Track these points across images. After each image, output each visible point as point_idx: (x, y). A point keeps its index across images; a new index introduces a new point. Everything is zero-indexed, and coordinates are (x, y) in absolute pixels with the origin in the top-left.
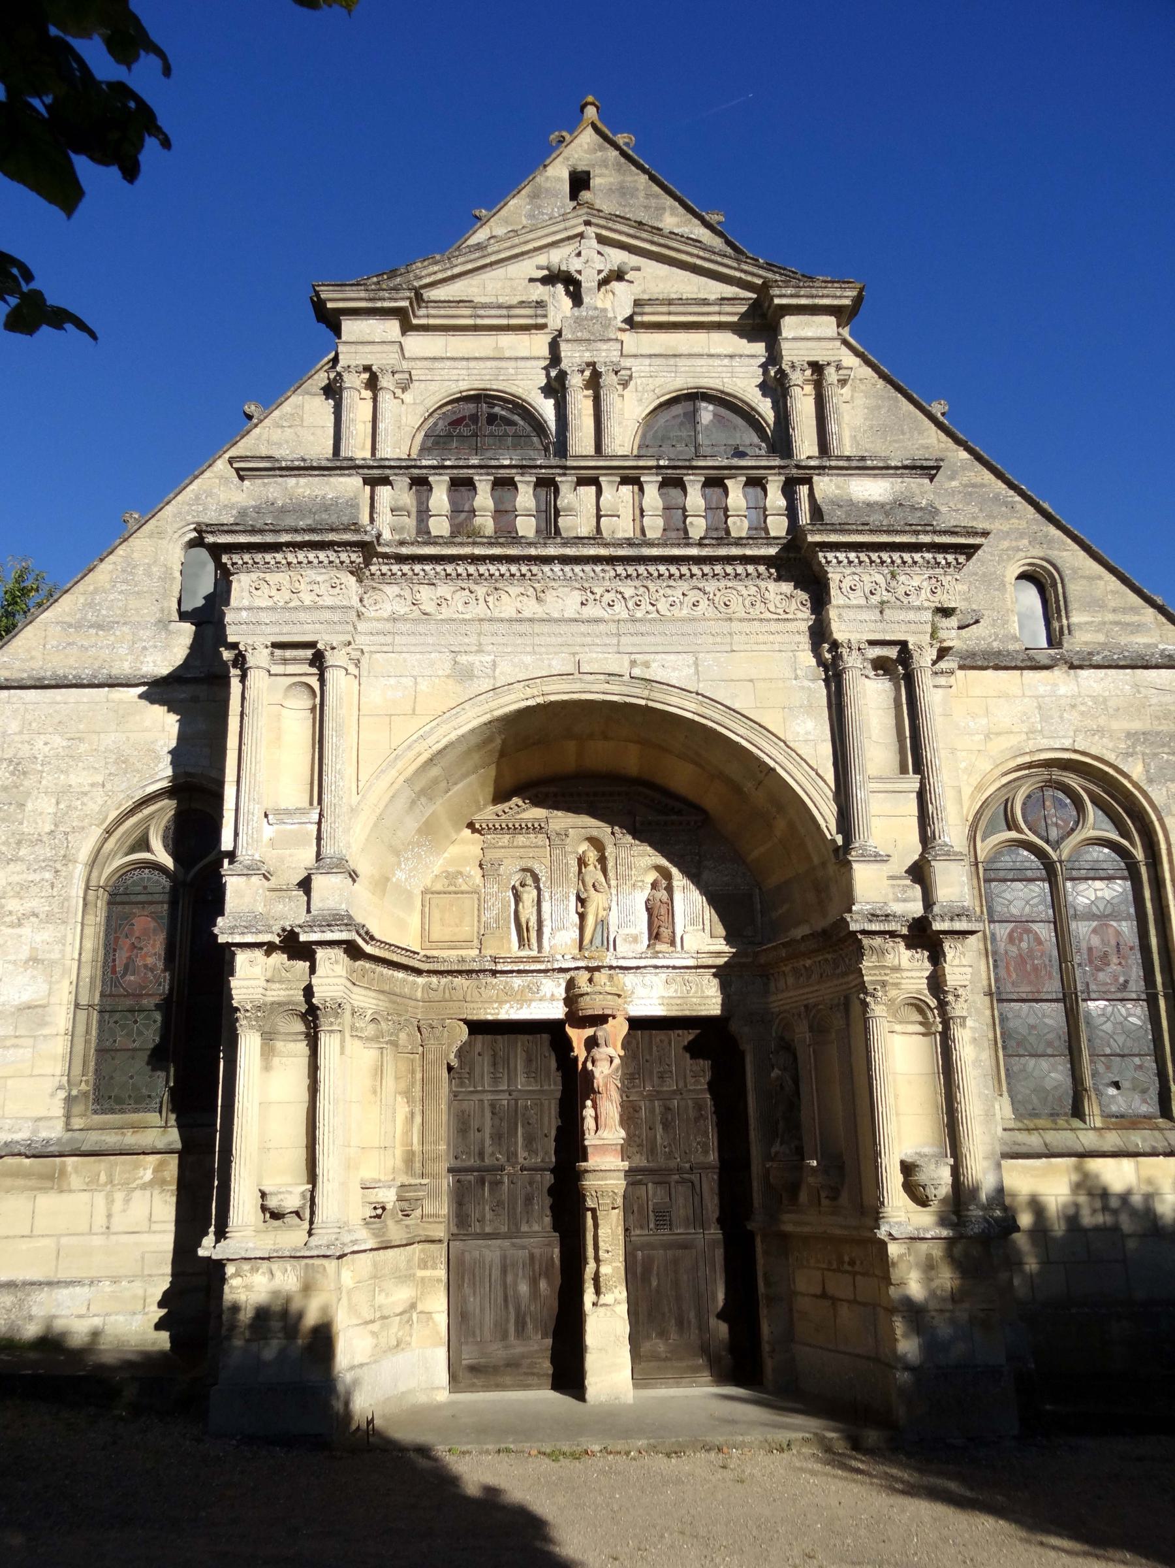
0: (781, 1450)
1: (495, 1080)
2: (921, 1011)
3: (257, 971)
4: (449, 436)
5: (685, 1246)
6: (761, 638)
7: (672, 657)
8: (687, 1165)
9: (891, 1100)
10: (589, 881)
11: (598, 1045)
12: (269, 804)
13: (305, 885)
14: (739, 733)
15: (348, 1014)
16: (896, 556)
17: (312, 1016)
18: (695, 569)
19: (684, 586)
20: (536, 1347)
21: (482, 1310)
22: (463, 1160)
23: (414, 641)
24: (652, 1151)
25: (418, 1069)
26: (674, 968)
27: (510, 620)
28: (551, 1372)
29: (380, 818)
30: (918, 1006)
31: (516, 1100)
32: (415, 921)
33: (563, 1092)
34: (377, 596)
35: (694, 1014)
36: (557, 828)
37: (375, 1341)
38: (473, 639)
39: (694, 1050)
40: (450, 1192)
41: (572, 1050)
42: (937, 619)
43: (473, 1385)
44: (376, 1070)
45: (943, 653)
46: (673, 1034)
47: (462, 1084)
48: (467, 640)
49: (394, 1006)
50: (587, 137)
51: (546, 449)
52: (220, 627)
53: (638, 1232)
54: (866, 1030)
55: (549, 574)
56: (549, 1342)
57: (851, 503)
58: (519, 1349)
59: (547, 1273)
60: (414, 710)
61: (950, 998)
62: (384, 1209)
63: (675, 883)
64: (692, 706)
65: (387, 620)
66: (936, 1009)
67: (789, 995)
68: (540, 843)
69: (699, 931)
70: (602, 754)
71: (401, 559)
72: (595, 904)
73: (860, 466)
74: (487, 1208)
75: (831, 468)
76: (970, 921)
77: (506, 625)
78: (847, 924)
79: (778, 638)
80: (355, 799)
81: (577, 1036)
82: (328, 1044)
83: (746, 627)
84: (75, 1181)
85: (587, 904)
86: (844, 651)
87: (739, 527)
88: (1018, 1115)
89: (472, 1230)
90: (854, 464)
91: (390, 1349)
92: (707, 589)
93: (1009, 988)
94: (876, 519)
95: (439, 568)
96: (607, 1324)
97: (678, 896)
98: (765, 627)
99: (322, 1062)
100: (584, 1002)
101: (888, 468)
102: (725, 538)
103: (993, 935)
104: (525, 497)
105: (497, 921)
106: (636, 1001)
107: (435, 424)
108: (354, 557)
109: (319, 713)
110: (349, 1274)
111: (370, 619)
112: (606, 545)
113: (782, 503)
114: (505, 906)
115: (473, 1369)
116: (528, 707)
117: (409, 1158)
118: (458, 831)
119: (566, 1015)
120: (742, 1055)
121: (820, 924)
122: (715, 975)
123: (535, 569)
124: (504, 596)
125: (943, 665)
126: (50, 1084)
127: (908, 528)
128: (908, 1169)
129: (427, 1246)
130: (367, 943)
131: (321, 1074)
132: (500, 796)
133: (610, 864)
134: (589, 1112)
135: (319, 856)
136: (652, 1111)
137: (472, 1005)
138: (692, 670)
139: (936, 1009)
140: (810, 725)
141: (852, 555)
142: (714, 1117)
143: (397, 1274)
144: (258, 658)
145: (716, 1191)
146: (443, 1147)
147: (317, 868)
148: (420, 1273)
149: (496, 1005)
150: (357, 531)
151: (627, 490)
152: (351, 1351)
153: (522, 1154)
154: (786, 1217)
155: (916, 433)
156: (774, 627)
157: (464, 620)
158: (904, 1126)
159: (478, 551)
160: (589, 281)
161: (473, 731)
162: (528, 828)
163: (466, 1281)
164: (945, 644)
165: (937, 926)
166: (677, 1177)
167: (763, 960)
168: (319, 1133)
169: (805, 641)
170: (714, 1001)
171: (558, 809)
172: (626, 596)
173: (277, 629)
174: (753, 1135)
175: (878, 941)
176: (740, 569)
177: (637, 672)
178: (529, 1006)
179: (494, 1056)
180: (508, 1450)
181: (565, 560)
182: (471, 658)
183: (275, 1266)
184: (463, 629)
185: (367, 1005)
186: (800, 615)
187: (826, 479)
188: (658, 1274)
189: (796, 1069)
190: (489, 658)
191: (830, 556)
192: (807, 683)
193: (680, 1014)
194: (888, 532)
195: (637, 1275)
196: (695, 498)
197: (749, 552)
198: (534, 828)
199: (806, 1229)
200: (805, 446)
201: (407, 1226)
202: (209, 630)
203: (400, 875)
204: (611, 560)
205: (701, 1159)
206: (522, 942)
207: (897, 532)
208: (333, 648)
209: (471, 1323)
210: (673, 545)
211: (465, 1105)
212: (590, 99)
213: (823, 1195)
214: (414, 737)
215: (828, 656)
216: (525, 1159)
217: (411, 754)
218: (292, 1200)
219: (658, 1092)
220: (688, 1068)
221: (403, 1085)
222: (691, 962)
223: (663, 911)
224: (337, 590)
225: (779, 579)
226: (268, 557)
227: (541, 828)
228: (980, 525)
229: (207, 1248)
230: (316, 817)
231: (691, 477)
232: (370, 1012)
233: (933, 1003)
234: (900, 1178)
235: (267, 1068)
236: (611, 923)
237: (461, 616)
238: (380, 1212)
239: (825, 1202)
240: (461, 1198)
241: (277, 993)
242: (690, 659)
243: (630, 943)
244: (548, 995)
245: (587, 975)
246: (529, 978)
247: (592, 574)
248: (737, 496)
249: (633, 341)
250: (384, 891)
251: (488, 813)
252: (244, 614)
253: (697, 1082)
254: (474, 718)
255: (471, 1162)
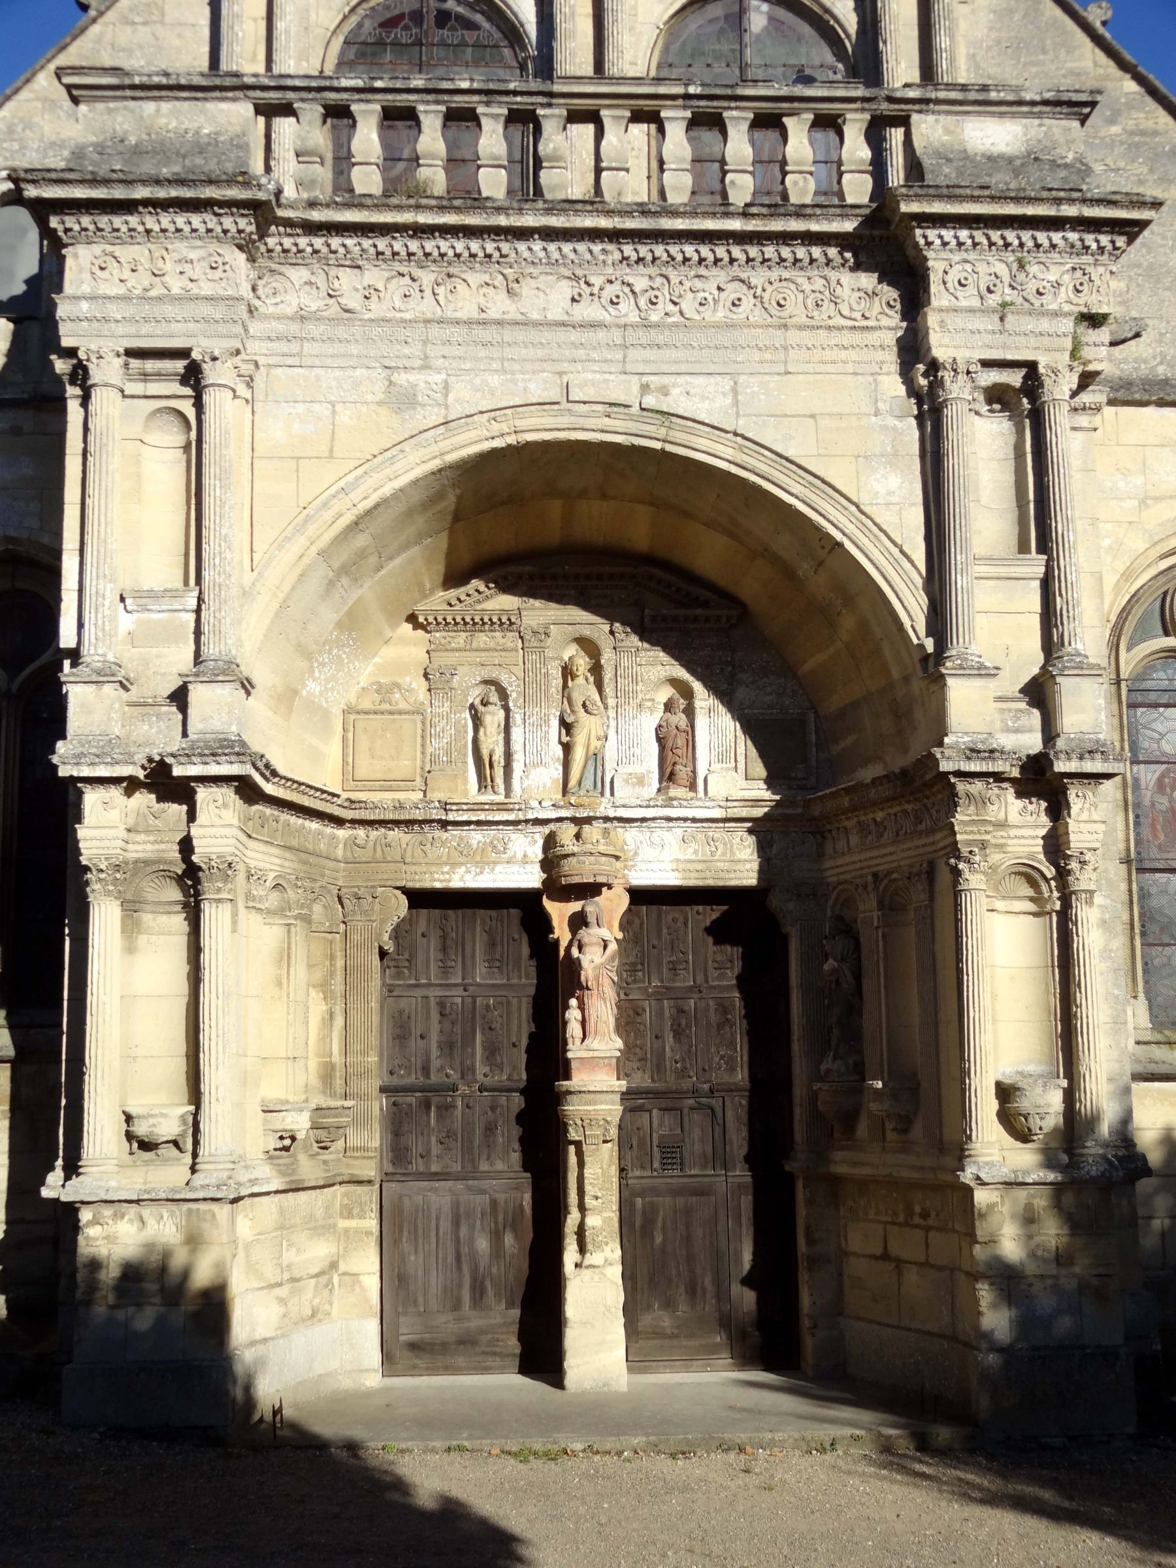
0: (823, 1450)
1: (445, 970)
2: (1032, 883)
3: (114, 816)
4: (380, 43)
5: (700, 1192)
6: (828, 355)
7: (701, 380)
8: (706, 1087)
9: (986, 1001)
10: (578, 699)
11: (586, 924)
12: (126, 583)
13: (180, 697)
14: (792, 492)
15: (241, 877)
16: (1026, 236)
17: (190, 878)
18: (737, 252)
19: (719, 276)
20: (498, 1320)
21: (426, 1271)
22: (402, 1077)
23: (331, 351)
24: (659, 1067)
25: (339, 954)
26: (694, 820)
27: (469, 323)
28: (518, 1351)
29: (284, 606)
30: (1030, 876)
31: (474, 998)
32: (334, 750)
33: (538, 987)
34: (276, 283)
35: (720, 883)
36: (534, 624)
37: (282, 1310)
38: (415, 350)
39: (719, 932)
40: (383, 1118)
41: (552, 931)
42: (1082, 328)
43: (415, 1367)
44: (281, 953)
45: (1087, 380)
46: (690, 911)
47: (399, 975)
48: (407, 351)
49: (305, 868)
51: (523, 67)
52: (50, 325)
53: (637, 1173)
54: (957, 907)
55: (526, 254)
56: (516, 1313)
57: (965, 156)
58: (476, 1322)
59: (514, 1225)
60: (331, 451)
61: (1074, 865)
62: (293, 1139)
63: (698, 704)
64: (728, 452)
65: (292, 319)
66: (1054, 881)
67: (851, 859)
68: (510, 645)
69: (730, 770)
70: (597, 520)
71: (312, 228)
72: (585, 731)
73: (980, 100)
74: (433, 1139)
75: (938, 102)
76: (1106, 760)
77: (464, 330)
78: (936, 762)
79: (853, 355)
80: (248, 578)
81: (559, 912)
82: (214, 917)
83: (807, 337)
85: (575, 731)
86: (946, 375)
87: (801, 189)
88: (1157, 1024)
89: (413, 1168)
90: (972, 96)
91: (303, 1320)
92: (754, 281)
93: (1154, 853)
94: (1000, 180)
95: (366, 243)
96: (594, 1291)
97: (701, 722)
98: (836, 338)
99: (206, 941)
100: (568, 866)
101: (1020, 103)
102: (779, 205)
103: (1136, 780)
104: (492, 139)
105: (448, 753)
106: (641, 866)
107: (360, 25)
108: (243, 223)
109: (195, 453)
110: (247, 1224)
111: (267, 317)
112: (609, 213)
113: (866, 153)
114: (462, 732)
115: (413, 1347)
116: (494, 452)
117: (327, 1074)
118: (394, 626)
119: (543, 883)
120: (785, 940)
121: (898, 762)
122: (750, 831)
123: (505, 247)
124: (461, 287)
125: (1086, 398)
127: (1045, 194)
128: (1005, 1093)
129: (352, 1188)
130: (267, 780)
131: (206, 958)
132: (455, 578)
133: (608, 676)
134: (573, 1014)
135: (198, 658)
136: (660, 1014)
137: (413, 868)
138: (729, 400)
139: (1054, 881)
140: (894, 481)
141: (964, 234)
142: (745, 1022)
143: (312, 1225)
144: (106, 371)
145: (745, 1119)
146: (373, 1059)
147: (197, 675)
148: (343, 1224)
149: (446, 869)
150: (246, 184)
151: (639, 131)
152: (252, 1322)
153: (481, 1069)
154: (839, 1155)
155: (1063, 52)
156: (847, 338)
157: (404, 321)
158: (1003, 1033)
159: (424, 218)
161: (415, 482)
162: (493, 623)
163: (406, 1234)
164: (1091, 368)
165: (1060, 766)
166: (691, 1102)
167: (817, 811)
168: (204, 1038)
169: (891, 360)
170: (748, 866)
171: (534, 596)
172: (637, 289)
173: (132, 330)
174: (796, 1047)
175: (978, 786)
176: (801, 252)
177: (650, 401)
178: (493, 870)
179: (444, 938)
180: (461, 1449)
181: (549, 234)
182: (412, 377)
183: (147, 1211)
184: (401, 334)
185: (268, 866)
186: (885, 322)
187: (931, 118)
188: (663, 1227)
189: (859, 959)
190: (439, 378)
191: (932, 234)
192: (891, 421)
193: (700, 883)
194: (1017, 200)
195: (634, 1228)
196: (739, 145)
197: (815, 227)
198: (502, 624)
199: (865, 1171)
200: (901, 67)
201: (325, 1162)
202: (34, 329)
203: (312, 687)
204: (615, 236)
205: (726, 1078)
206: (484, 782)
207: (1030, 200)
208: (214, 359)
209: (412, 1287)
210: (706, 215)
211: (403, 1003)
213: (889, 1126)
214: (332, 491)
215: (923, 382)
216: (485, 1075)
217: (328, 515)
218: (167, 1123)
219: (667, 988)
220: (710, 955)
221: (318, 975)
222: (718, 813)
223: (680, 742)
224: (218, 274)
225: (857, 267)
226: (118, 221)
227: (511, 624)
228: (1151, 192)
229: (54, 1186)
230: (192, 603)
231: (735, 113)
232: (272, 875)
233: (1050, 872)
234: (994, 1105)
235: (130, 948)
236: (607, 758)
237: (398, 315)
238: (288, 1143)
239: (891, 1136)
240: (398, 1125)
241: (142, 848)
242: (726, 384)
243: (633, 785)
244: (519, 856)
245: (572, 829)
246: (492, 832)
247: (588, 256)
248: (800, 142)
250: (290, 709)
251: (437, 601)
252: (84, 305)
253: (722, 976)
254: (417, 464)
255: (411, 1080)
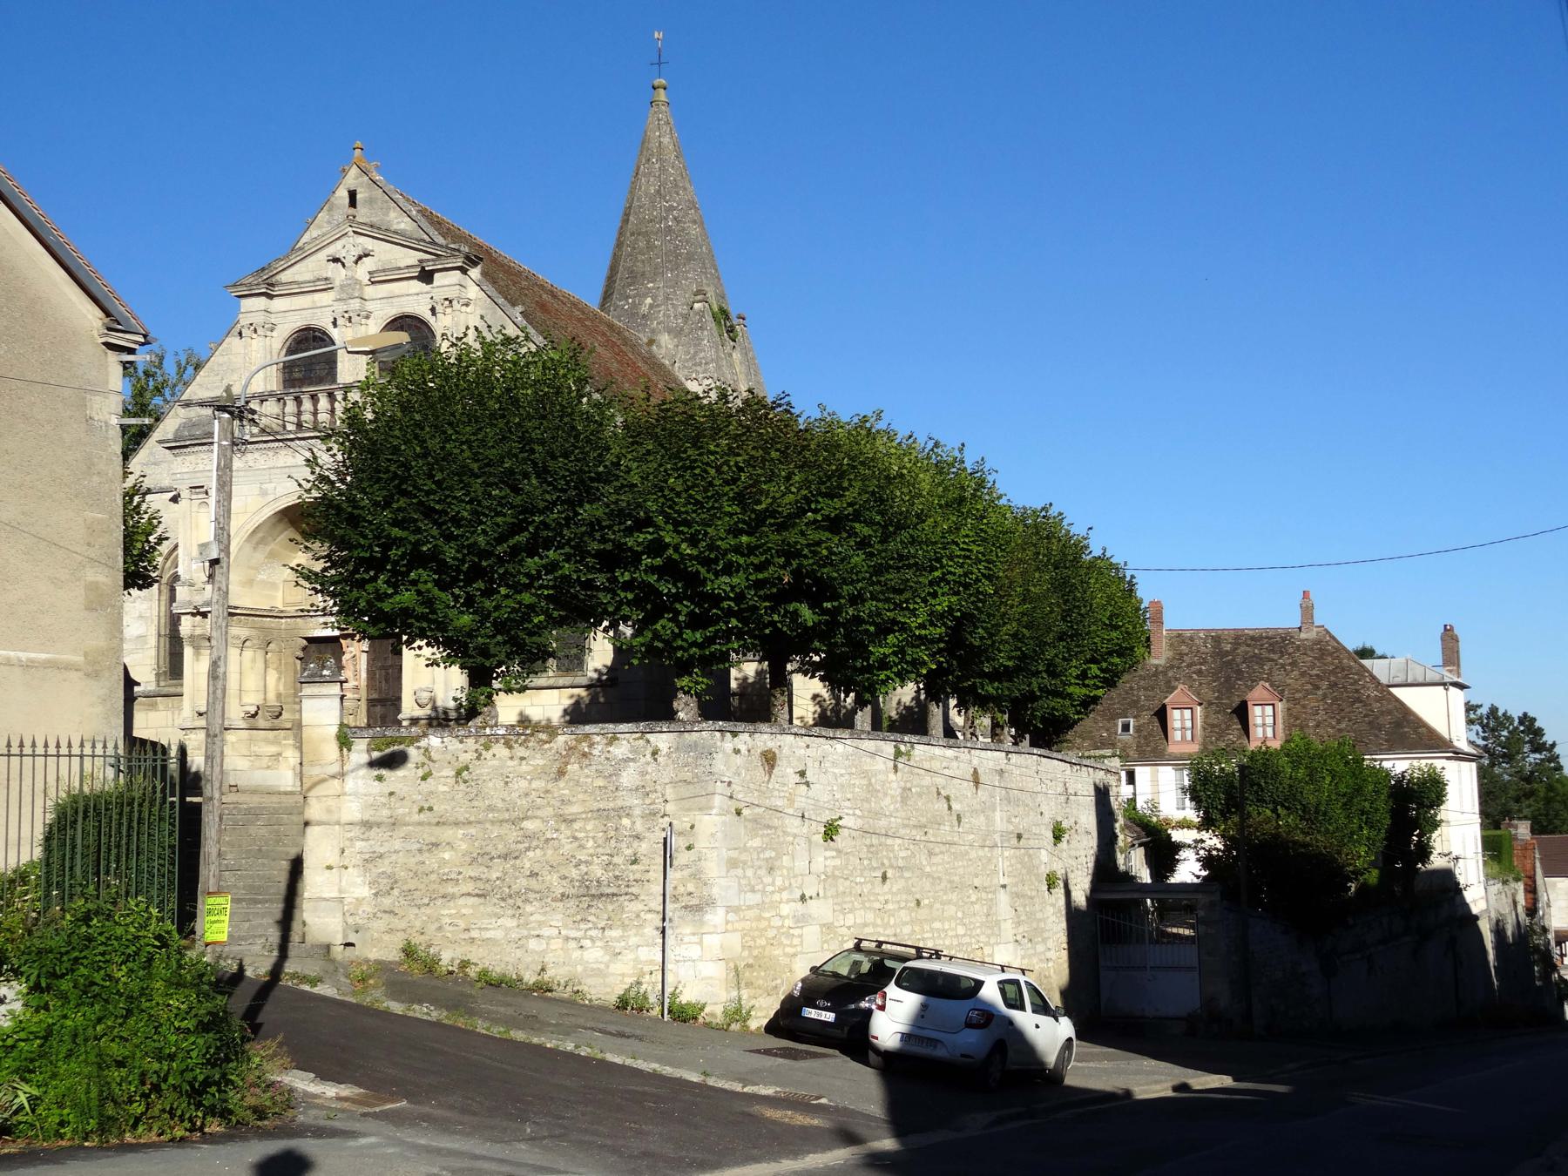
32: (280, 594)
50: (354, 171)
84: (161, 707)
126: (149, 669)
160: (349, 261)
212: (358, 144)
249: (370, 291)
254: (268, 512)
